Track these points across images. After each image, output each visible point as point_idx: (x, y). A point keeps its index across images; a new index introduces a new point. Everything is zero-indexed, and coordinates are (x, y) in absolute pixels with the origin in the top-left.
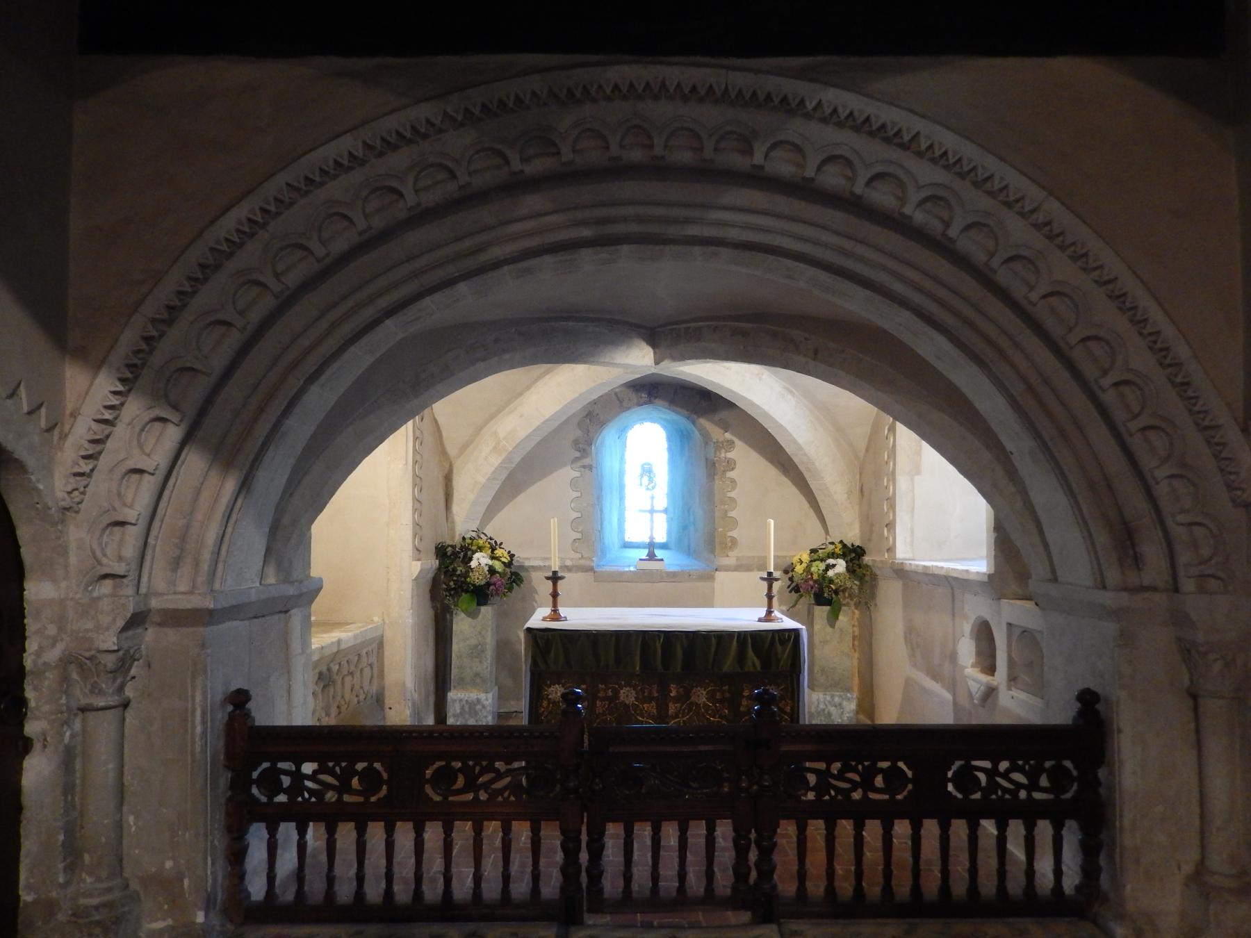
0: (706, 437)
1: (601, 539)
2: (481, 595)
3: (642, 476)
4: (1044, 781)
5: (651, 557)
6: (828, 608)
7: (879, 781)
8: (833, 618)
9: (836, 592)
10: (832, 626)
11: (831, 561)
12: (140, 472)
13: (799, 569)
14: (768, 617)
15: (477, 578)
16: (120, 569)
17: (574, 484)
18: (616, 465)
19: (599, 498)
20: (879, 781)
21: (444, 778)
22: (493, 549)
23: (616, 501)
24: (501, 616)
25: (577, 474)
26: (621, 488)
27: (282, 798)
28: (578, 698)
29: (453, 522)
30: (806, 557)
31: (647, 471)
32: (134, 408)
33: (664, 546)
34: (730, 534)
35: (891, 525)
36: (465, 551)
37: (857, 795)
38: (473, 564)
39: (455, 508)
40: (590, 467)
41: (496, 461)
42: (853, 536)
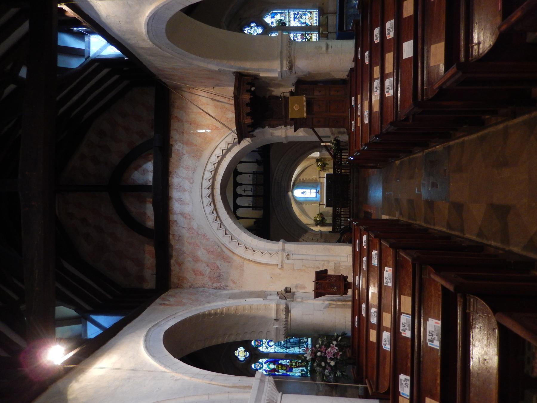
0: (298, 183)
1: (315, 201)
2: (323, 219)
3: (304, 194)
4: (338, 154)
5: (318, 192)
6: (326, 165)
7: (338, 170)
8: (327, 164)
9: (324, 163)
10: (329, 164)
11: (319, 165)
12: (308, 238)
13: (320, 169)
14: (325, 177)
15: (321, 219)
16: (317, 240)
17: (306, 205)
18: (302, 198)
19: (308, 201)
20: (338, 170)
21: (338, 212)
22: (316, 217)
23: (308, 198)
24: (327, 216)
25: (304, 204)
26: (306, 198)
27: (339, 228)
28: (330, 199)
29: (312, 224)
30: (318, 168)
31: (303, 193)
32: (302, 238)
33: (316, 190)
34: (314, 179)
35: (313, 157)
36: (316, 221)
37: (340, 172)
38: (318, 220)
39: (310, 223)
40: (303, 202)
41: (302, 216)
42: (315, 160)
